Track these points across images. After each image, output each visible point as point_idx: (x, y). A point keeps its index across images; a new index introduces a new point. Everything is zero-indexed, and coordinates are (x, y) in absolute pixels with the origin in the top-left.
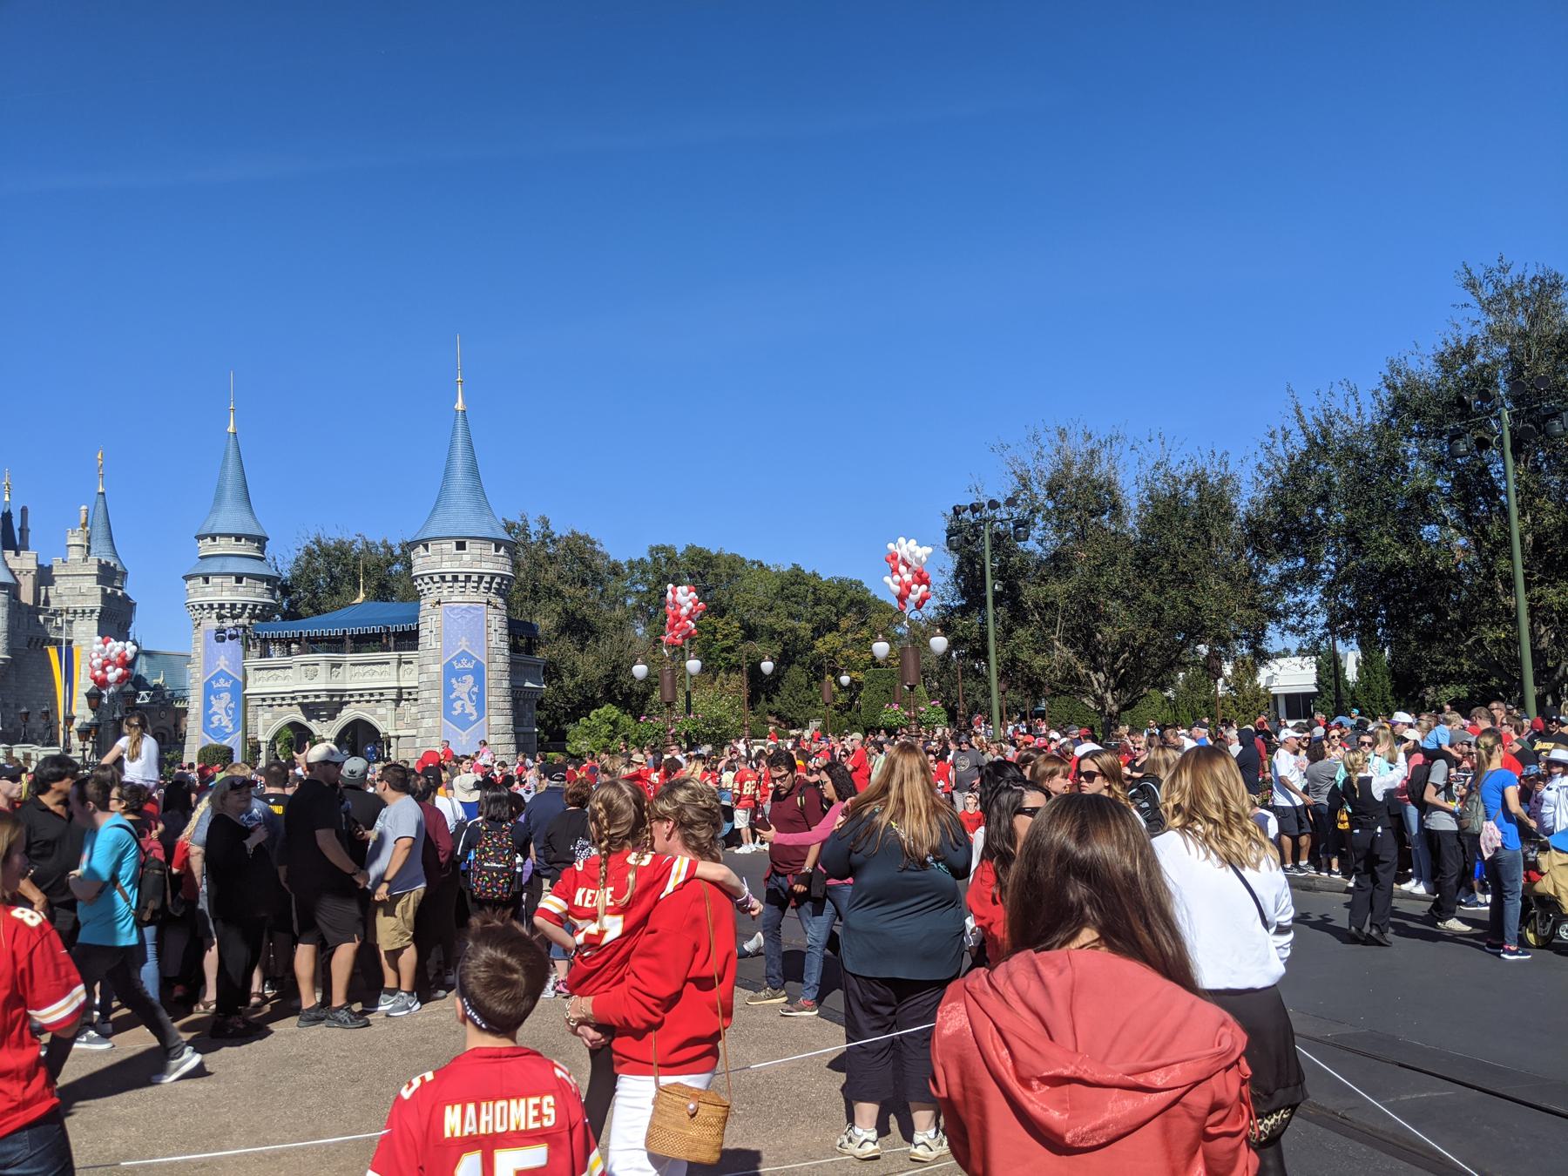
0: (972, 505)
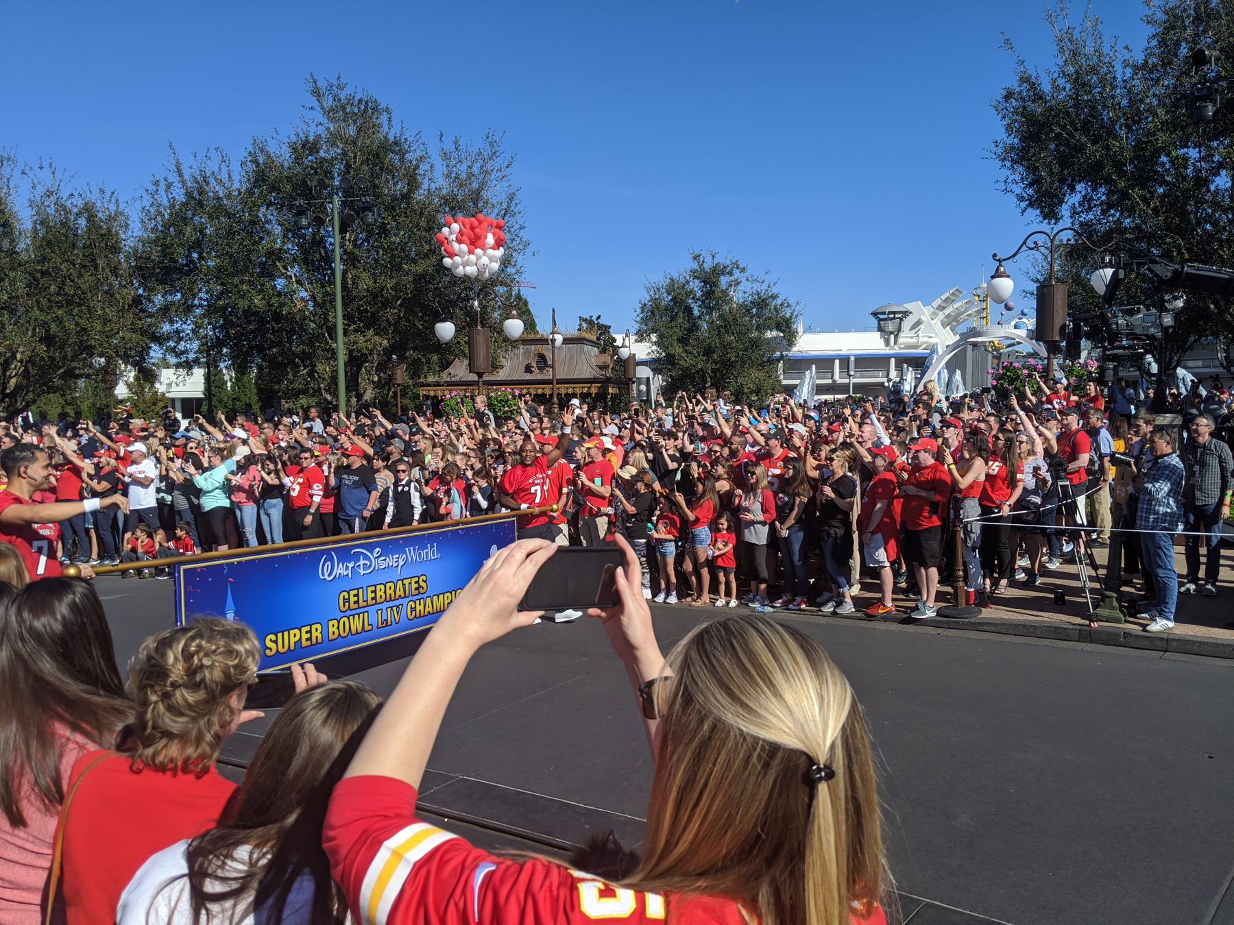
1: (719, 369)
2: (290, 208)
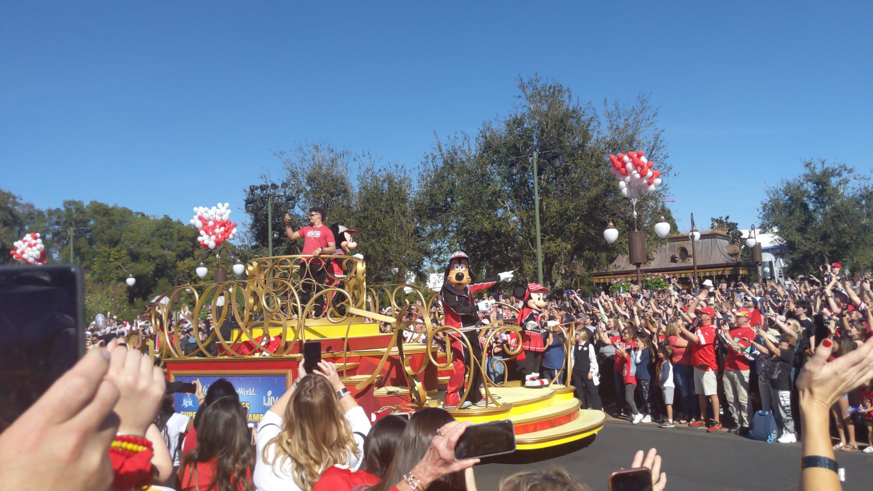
0: (261, 186)
1: (835, 251)
2: (506, 163)
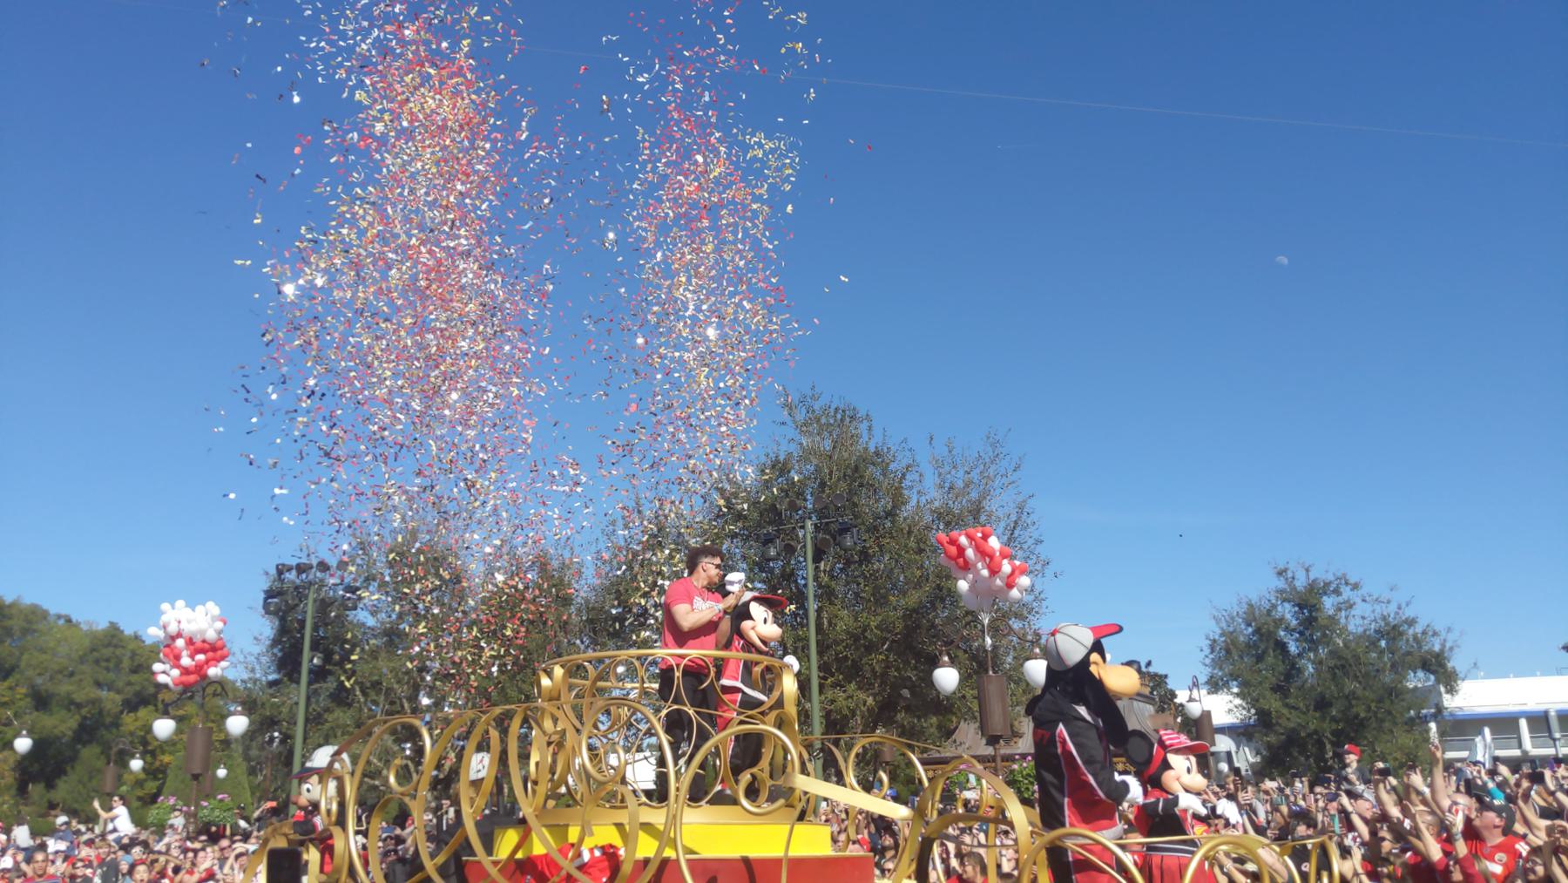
1: (1342, 731)
